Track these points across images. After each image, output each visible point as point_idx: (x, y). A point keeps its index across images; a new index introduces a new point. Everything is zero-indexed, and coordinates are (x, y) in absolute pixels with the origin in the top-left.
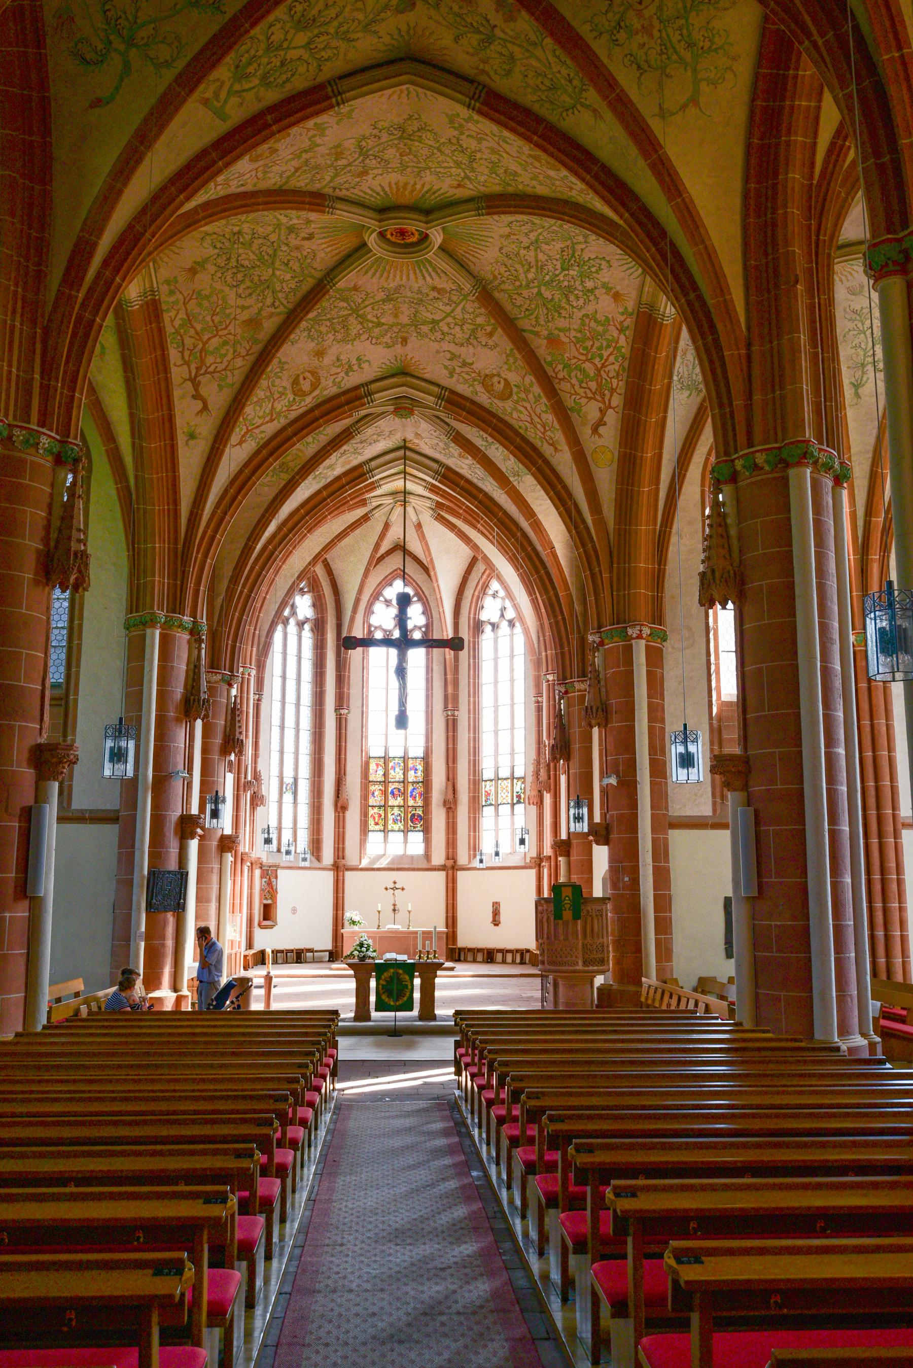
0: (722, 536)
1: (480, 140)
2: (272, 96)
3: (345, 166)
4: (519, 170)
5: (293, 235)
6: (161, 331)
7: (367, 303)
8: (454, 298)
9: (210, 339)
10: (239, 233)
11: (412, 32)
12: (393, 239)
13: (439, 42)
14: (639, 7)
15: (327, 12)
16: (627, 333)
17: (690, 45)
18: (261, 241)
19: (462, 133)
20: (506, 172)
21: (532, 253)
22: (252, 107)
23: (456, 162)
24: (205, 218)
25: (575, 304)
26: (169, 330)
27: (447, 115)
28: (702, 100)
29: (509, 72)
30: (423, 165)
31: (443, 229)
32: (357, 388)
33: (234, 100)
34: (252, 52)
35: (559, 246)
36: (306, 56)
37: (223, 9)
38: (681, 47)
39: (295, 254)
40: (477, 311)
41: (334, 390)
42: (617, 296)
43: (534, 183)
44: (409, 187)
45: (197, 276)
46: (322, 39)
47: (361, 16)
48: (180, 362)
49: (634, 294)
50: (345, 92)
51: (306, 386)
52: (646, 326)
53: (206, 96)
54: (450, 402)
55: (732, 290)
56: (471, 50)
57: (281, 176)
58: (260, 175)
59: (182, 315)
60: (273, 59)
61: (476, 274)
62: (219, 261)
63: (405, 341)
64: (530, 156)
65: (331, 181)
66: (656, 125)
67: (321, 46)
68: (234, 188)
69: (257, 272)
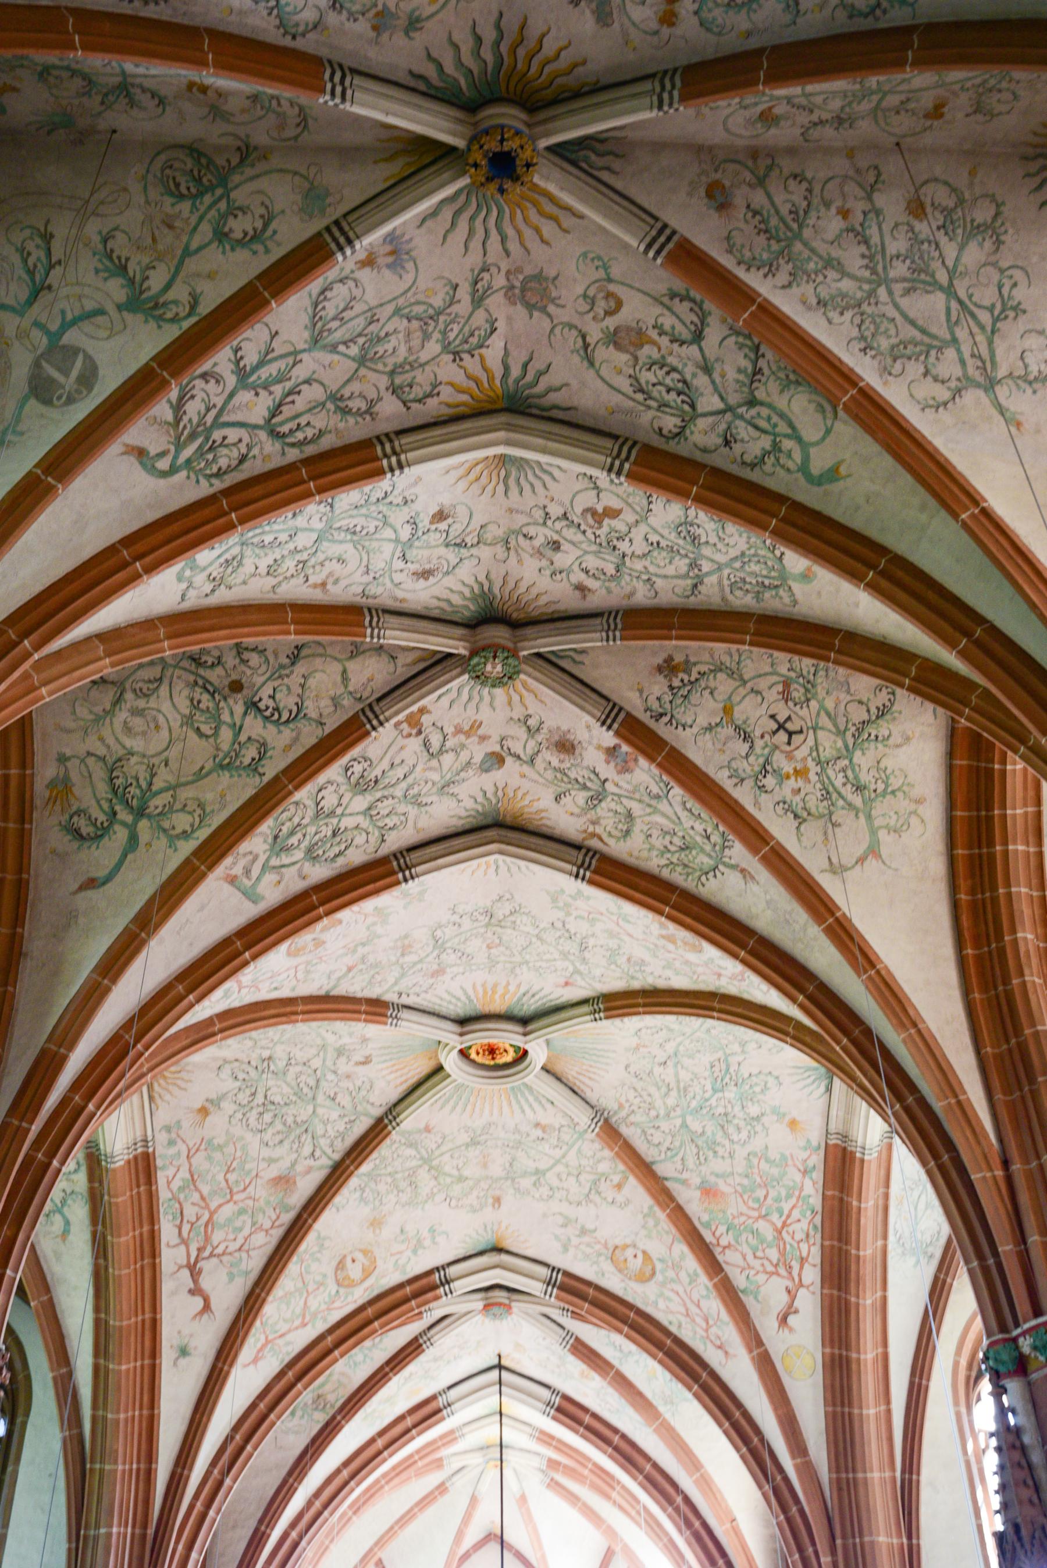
0: (1019, 1464)
1: (593, 922)
2: (319, 873)
3: (415, 964)
4: (647, 957)
5: (343, 1059)
6: (152, 1197)
7: (443, 1149)
8: (566, 1137)
9: (220, 1206)
10: (270, 1058)
11: (500, 793)
12: (479, 1059)
13: (535, 804)
14: (788, 748)
15: (391, 773)
16: (814, 1175)
17: (859, 788)
18: (298, 1068)
19: (568, 914)
20: (629, 960)
21: (670, 1070)
22: (292, 884)
24: (221, 1031)
25: (735, 1137)
26: (164, 1194)
27: (548, 893)
28: (884, 851)
29: (628, 832)
30: (518, 959)
31: (548, 1042)
32: (429, 1273)
33: (270, 878)
34: (296, 820)
35: (706, 1059)
36: (365, 823)
37: (261, 770)
38: (847, 791)
39: (345, 1084)
40: (599, 1155)
41: (394, 1278)
42: (793, 1124)
43: (668, 973)
44: (500, 990)
45: (208, 1119)
46: (386, 802)
47: (435, 776)
48: (176, 1240)
49: (818, 1122)
50: (415, 866)
51: (354, 1271)
52: (842, 1166)
53: (233, 872)
54: (563, 1288)
55: (967, 1087)
56: (577, 811)
57: (329, 977)
58: (300, 975)
59: (184, 1173)
60: (324, 828)
61: (594, 1102)
62: (241, 1096)
63: (498, 1200)
64: (663, 937)
65: (396, 983)
66: (828, 883)
67: (386, 812)
68: (265, 994)
69: (291, 1110)
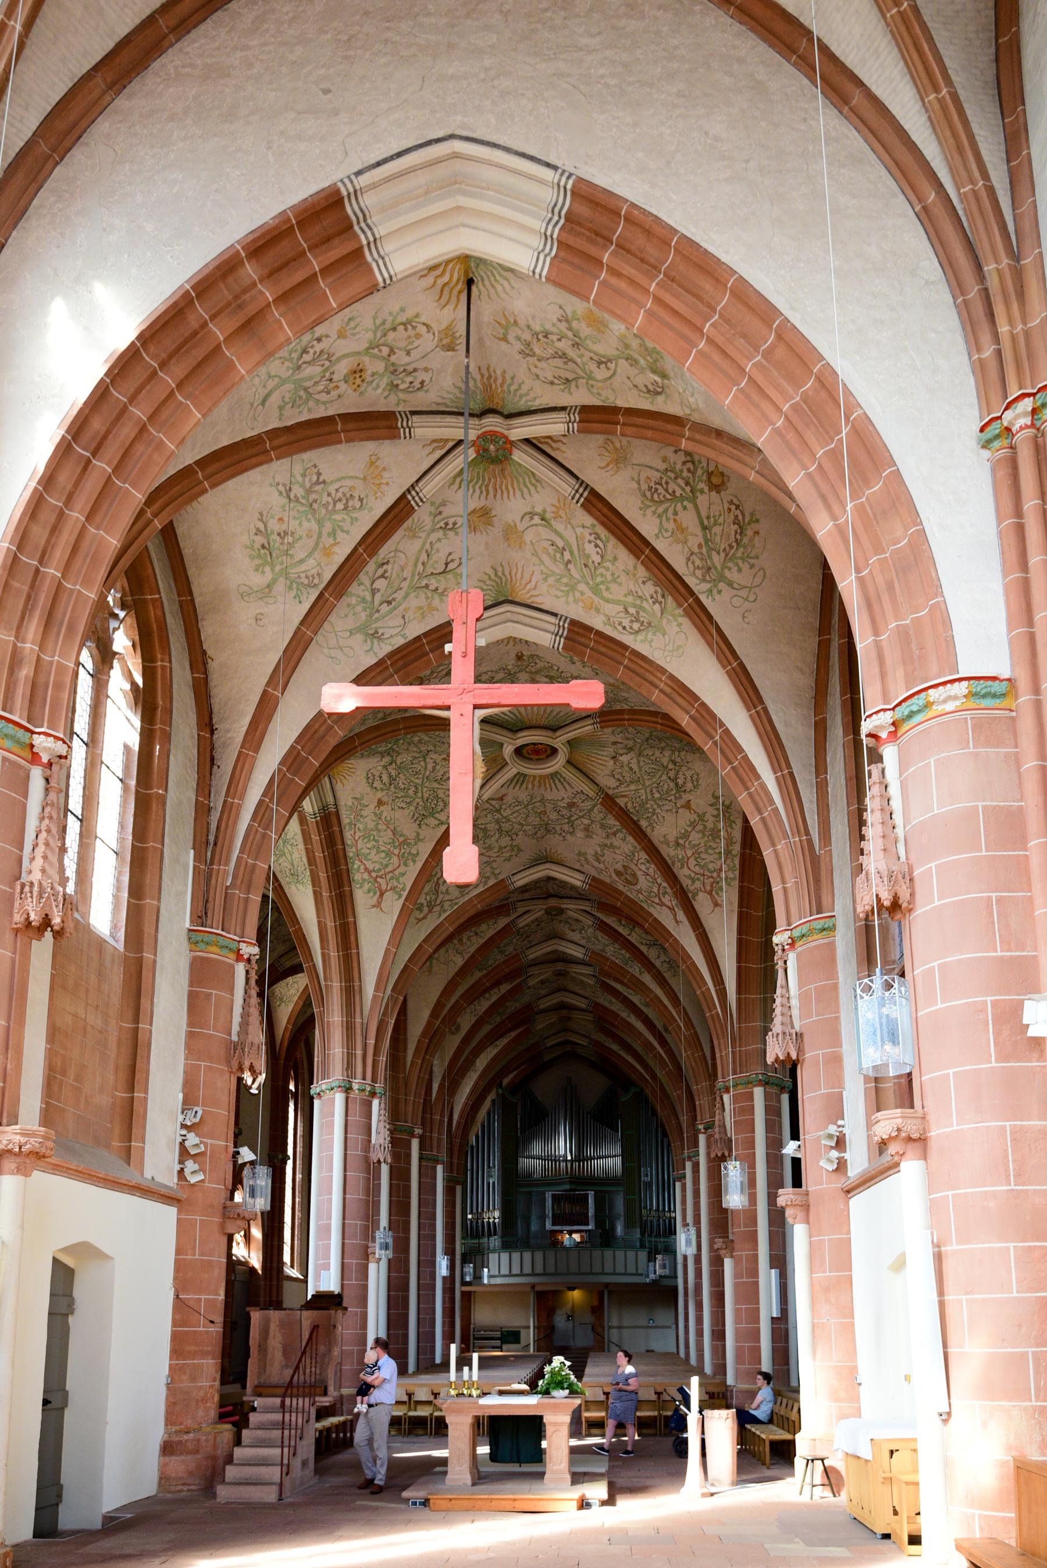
1: (501, 848)
19: (511, 845)
23: (509, 821)
